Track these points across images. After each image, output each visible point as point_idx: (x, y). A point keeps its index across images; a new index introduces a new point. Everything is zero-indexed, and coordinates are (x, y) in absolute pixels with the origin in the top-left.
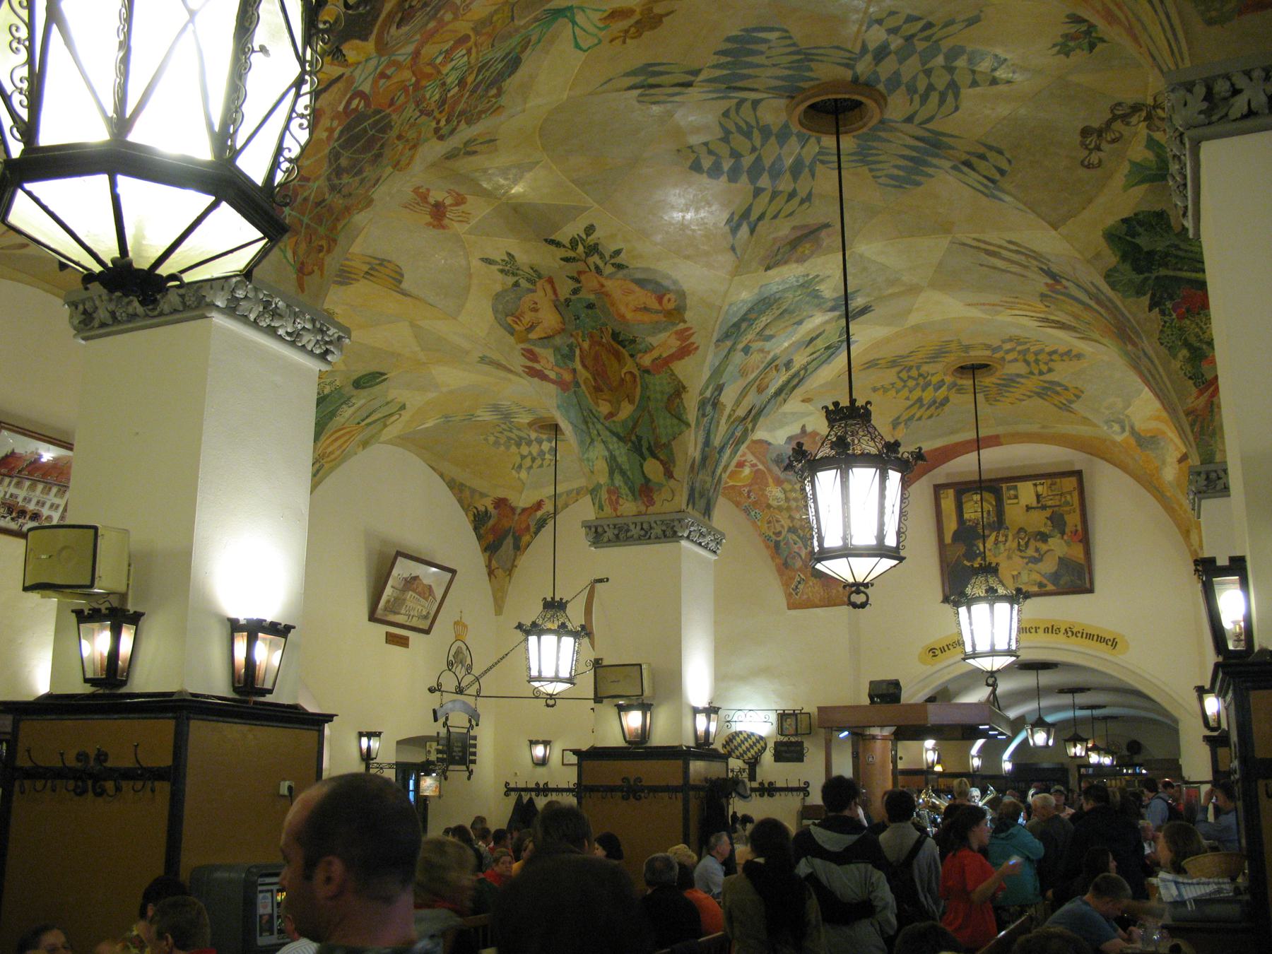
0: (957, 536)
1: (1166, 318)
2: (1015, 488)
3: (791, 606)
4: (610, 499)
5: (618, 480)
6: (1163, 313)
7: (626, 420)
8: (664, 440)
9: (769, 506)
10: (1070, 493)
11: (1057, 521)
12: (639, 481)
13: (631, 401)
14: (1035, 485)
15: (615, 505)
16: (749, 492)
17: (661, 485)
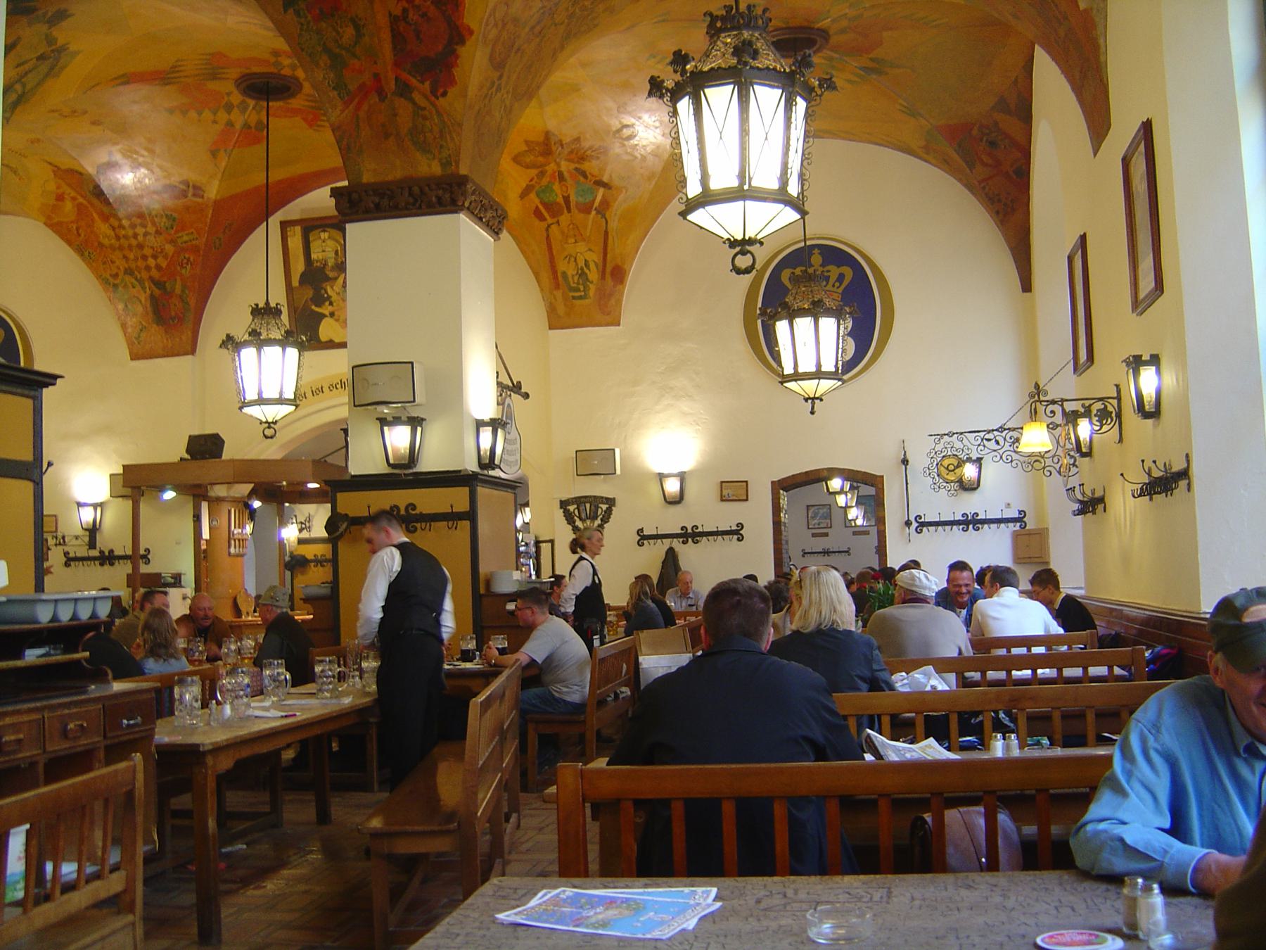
0: (304, 278)
1: (302, 20)
3: (135, 357)
6: (297, 13)
9: (101, 245)
16: (77, 229)
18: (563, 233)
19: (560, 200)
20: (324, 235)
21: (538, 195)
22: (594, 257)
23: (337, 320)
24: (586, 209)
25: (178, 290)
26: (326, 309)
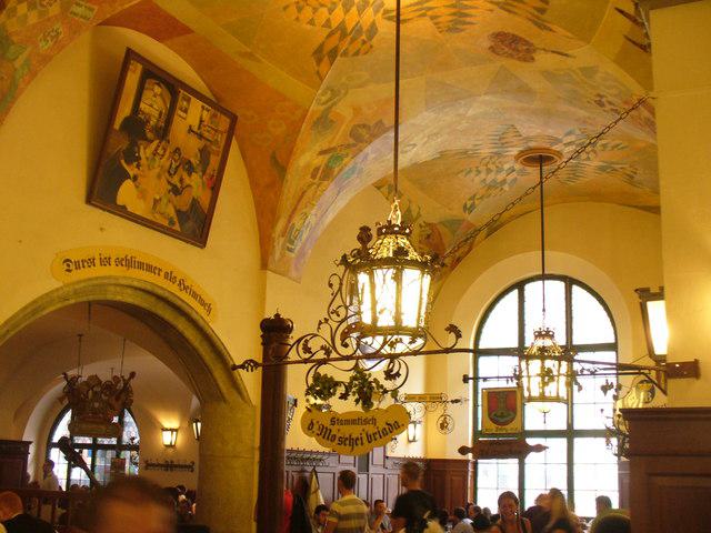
2: (189, 101)
10: (222, 133)
11: (204, 154)
14: (203, 107)
20: (158, 90)
23: (137, 187)
25: (17, 64)
26: (132, 170)
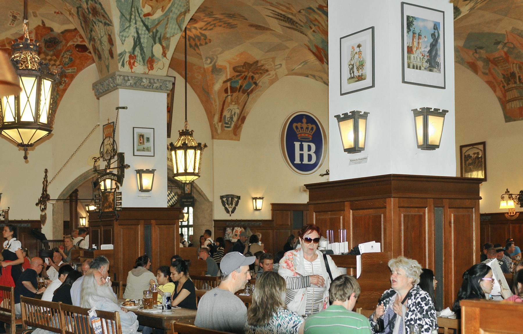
4: (130, 63)
5: (137, 51)
7: (155, 20)
8: (168, 36)
12: (148, 55)
13: (163, 10)
15: (131, 65)
17: (160, 60)
18: (231, 100)
19: (238, 87)
21: (231, 83)
22: (238, 111)
24: (244, 92)
